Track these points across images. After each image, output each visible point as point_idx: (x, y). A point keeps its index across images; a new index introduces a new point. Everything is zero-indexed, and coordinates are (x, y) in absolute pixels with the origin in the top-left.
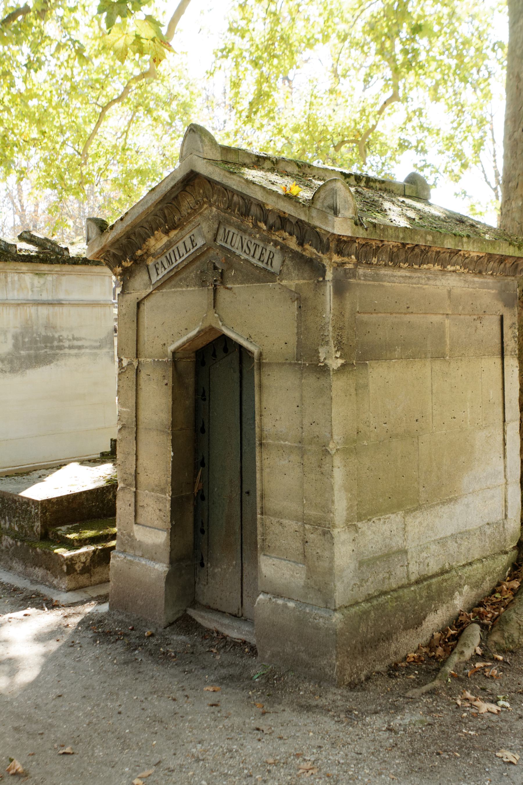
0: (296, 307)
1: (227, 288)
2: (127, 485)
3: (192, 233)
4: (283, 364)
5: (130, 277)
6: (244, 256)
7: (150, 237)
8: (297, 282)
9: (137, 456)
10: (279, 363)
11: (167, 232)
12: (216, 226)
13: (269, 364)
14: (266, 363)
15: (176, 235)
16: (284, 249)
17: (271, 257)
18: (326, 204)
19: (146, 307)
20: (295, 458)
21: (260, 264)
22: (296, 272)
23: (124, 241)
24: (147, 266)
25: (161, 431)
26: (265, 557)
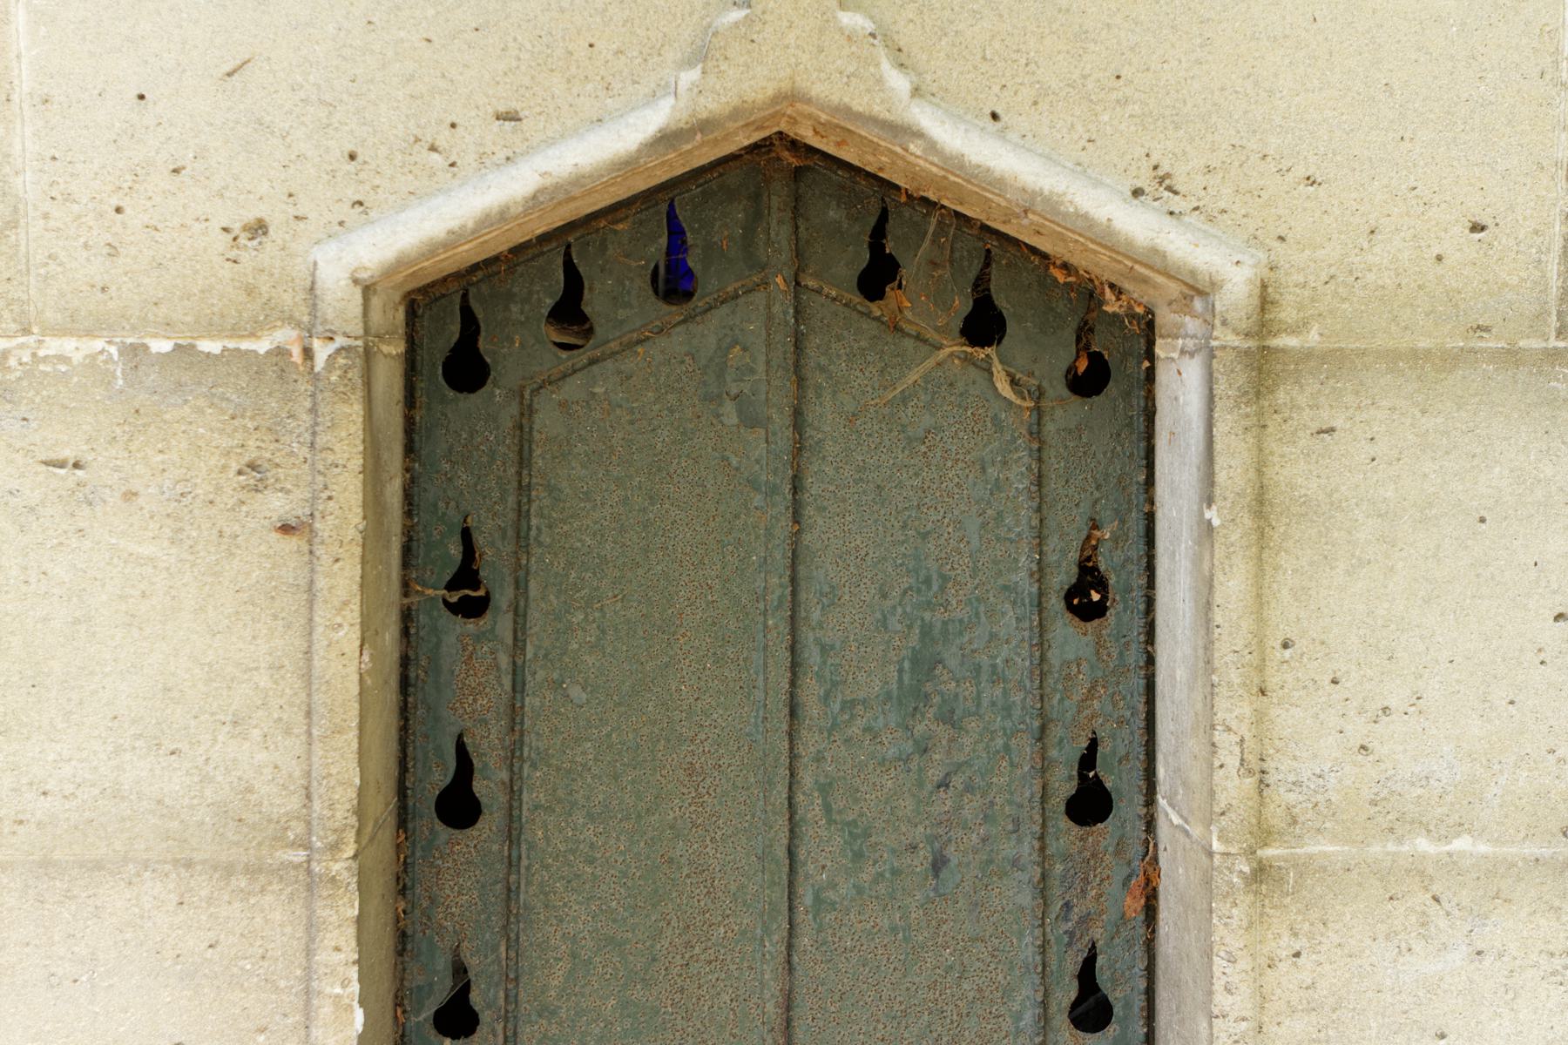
4: (1451, 360)
10: (1415, 355)
13: (1334, 362)
14: (1307, 355)
25: (252, 871)
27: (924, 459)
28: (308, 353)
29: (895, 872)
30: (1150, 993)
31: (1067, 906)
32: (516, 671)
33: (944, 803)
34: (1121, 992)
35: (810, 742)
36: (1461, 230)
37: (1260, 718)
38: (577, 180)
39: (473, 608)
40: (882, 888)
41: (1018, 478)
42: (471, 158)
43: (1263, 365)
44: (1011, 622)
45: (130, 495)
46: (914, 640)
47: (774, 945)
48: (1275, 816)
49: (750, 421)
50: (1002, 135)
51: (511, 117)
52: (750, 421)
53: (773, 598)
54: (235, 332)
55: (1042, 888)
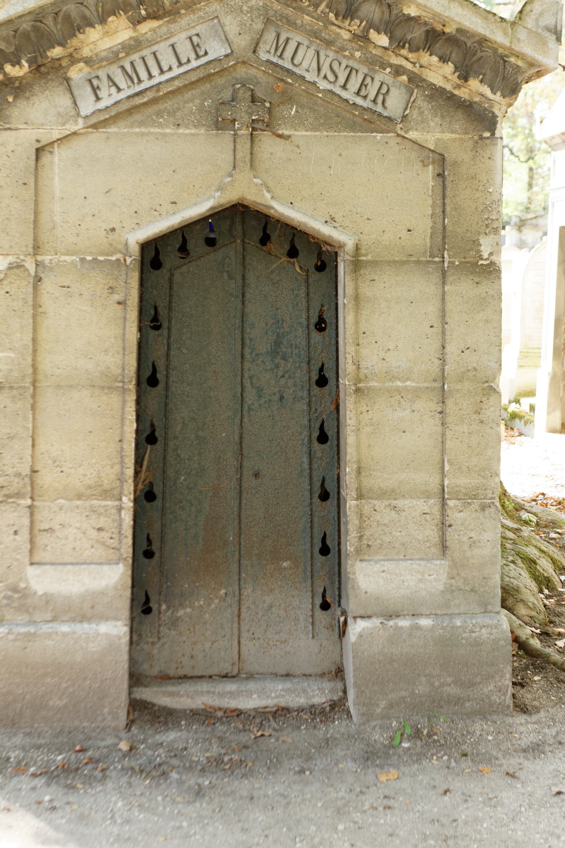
0: (430, 174)
1: (280, 136)
2: (8, 496)
3: (194, 32)
4: (403, 263)
5: (15, 98)
6: (323, 85)
7: (92, 25)
8: (439, 136)
9: (33, 440)
10: (394, 262)
11: (136, 22)
12: (259, 26)
13: (375, 263)
14: (368, 261)
15: (154, 30)
16: (416, 81)
17: (384, 90)
18: (542, 23)
19: (57, 159)
20: (427, 405)
21: (359, 101)
22: (438, 120)
23: (26, 26)
24: (68, 80)
25: (109, 388)
26: (364, 564)
27: (277, 289)
28: (125, 260)
29: (270, 400)
30: (338, 432)
31: (316, 409)
32: (168, 345)
33: (283, 381)
34: (331, 433)
35: (247, 365)
36: (405, 231)
37: (357, 352)
38: (190, 219)
39: (157, 328)
40: (266, 405)
41: (303, 295)
42: (165, 213)
43: (357, 265)
44: (301, 332)
45: (81, 295)
46: (275, 337)
47: (237, 420)
48: (362, 376)
49: (231, 278)
50: (293, 208)
51: (174, 203)
52: (231, 278)
53: (237, 326)
54: (107, 255)
55: (309, 404)
